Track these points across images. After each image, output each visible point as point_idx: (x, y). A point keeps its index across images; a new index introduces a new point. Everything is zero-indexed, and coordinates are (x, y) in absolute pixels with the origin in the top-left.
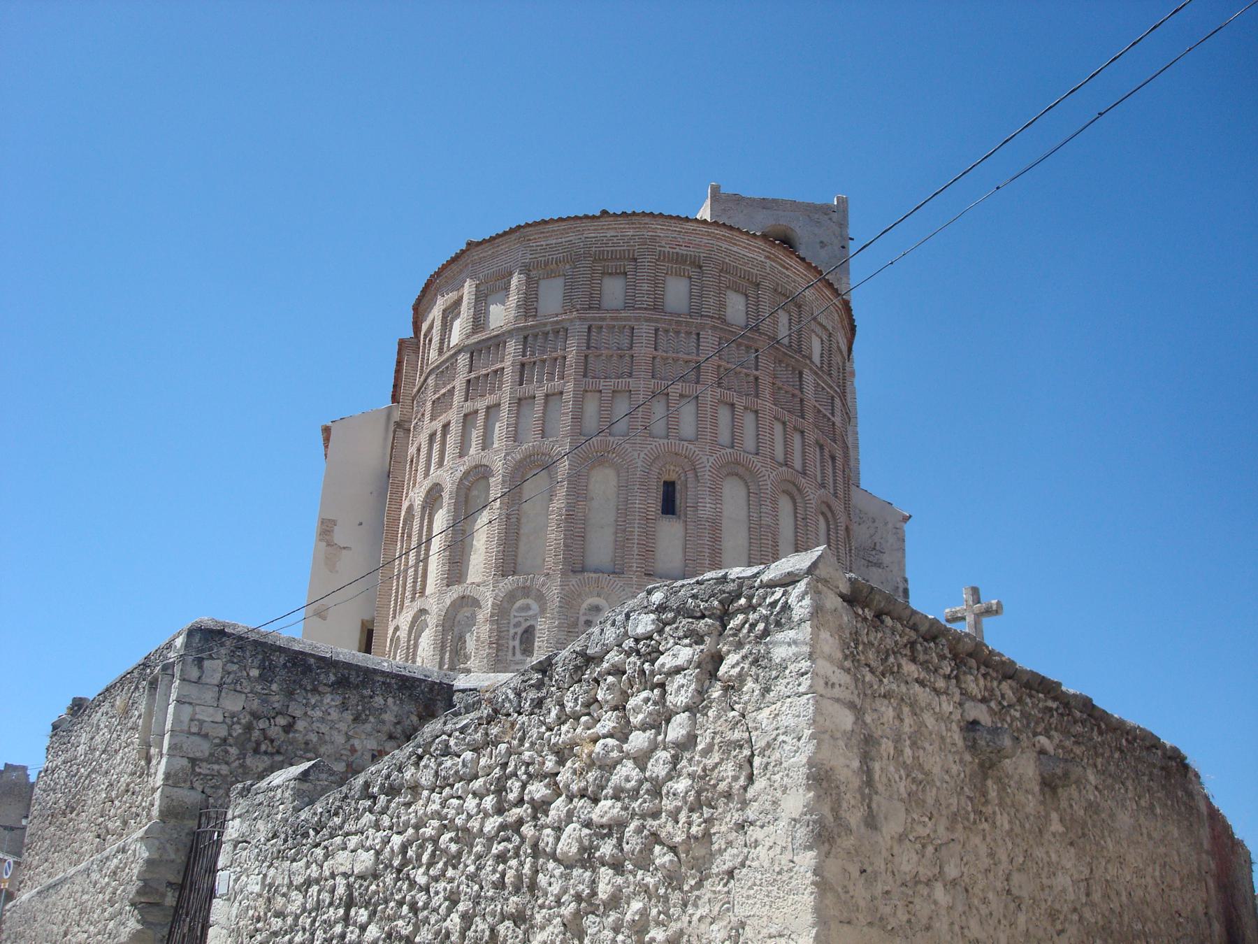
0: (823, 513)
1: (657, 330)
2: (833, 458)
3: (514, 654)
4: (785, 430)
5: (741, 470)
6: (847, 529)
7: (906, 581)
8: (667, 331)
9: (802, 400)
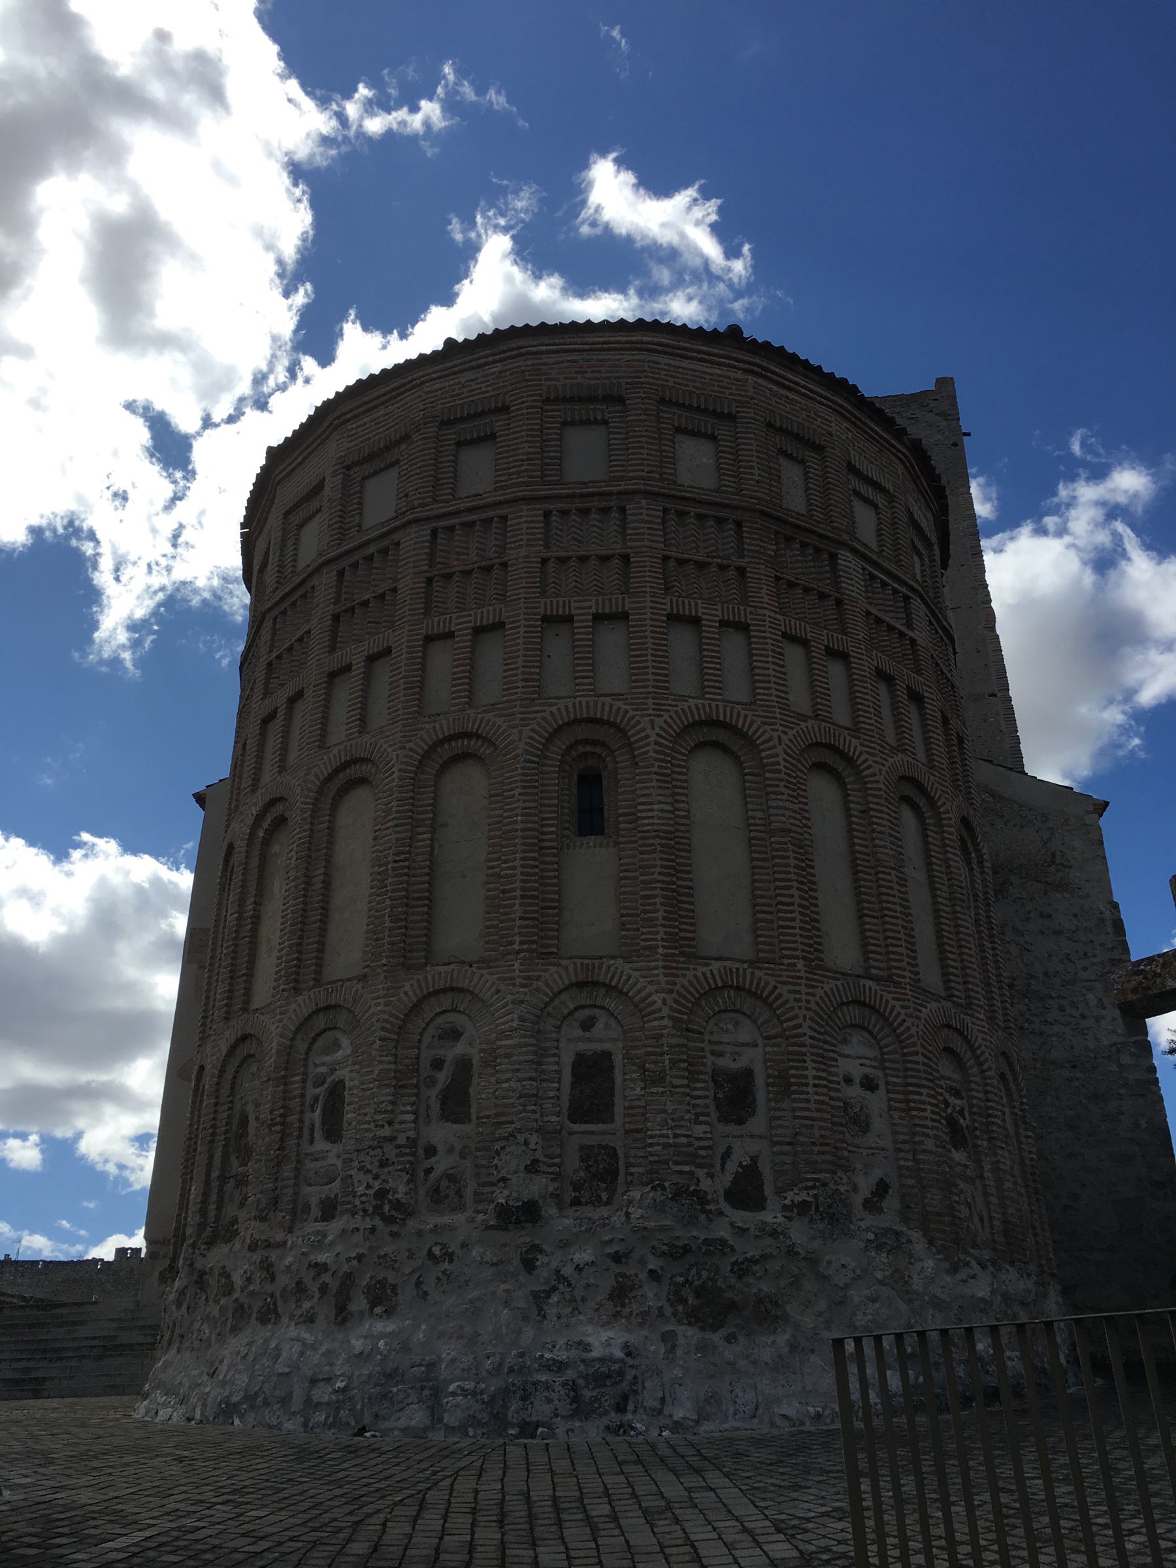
0: (905, 799)
1: (547, 514)
2: (917, 698)
3: (312, 1141)
4: (809, 657)
5: (721, 736)
6: (965, 821)
7: (1116, 906)
8: (565, 513)
9: (839, 603)
